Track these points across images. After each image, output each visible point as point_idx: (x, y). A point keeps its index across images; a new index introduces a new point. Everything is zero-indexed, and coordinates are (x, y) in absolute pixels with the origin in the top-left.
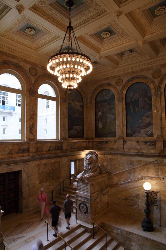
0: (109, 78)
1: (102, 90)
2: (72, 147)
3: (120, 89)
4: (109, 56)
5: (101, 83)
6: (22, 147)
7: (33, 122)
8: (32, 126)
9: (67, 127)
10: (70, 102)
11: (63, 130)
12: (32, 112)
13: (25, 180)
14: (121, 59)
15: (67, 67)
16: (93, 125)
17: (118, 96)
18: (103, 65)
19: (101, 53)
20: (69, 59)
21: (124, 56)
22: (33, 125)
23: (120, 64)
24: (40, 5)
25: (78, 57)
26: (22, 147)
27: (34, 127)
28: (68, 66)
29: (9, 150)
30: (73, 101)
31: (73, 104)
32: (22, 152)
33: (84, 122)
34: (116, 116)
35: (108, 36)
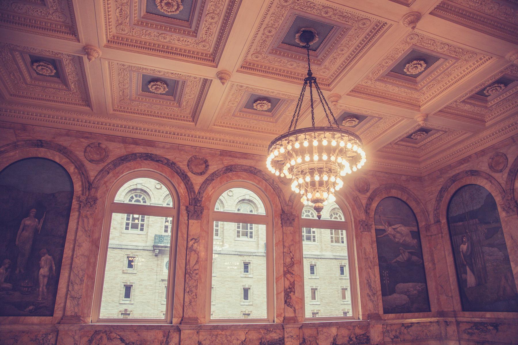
0: (470, 157)
1: (460, 189)
2: (396, 337)
3: (505, 179)
4: (445, 108)
5: (454, 173)
6: (268, 337)
7: (292, 281)
8: (290, 288)
9: (377, 285)
10: (381, 227)
11: (370, 296)
12: (288, 260)
14: (486, 107)
15: (304, 162)
16: (451, 279)
17: (503, 199)
18: (446, 132)
19: (422, 108)
20: (306, 144)
21: (488, 98)
22: (291, 287)
23: (486, 120)
24: (257, 59)
25: (325, 137)
26: (268, 337)
27: (294, 292)
28: (307, 158)
30: (390, 225)
31: (390, 230)
33: (426, 271)
34: (509, 250)
35: (420, 69)
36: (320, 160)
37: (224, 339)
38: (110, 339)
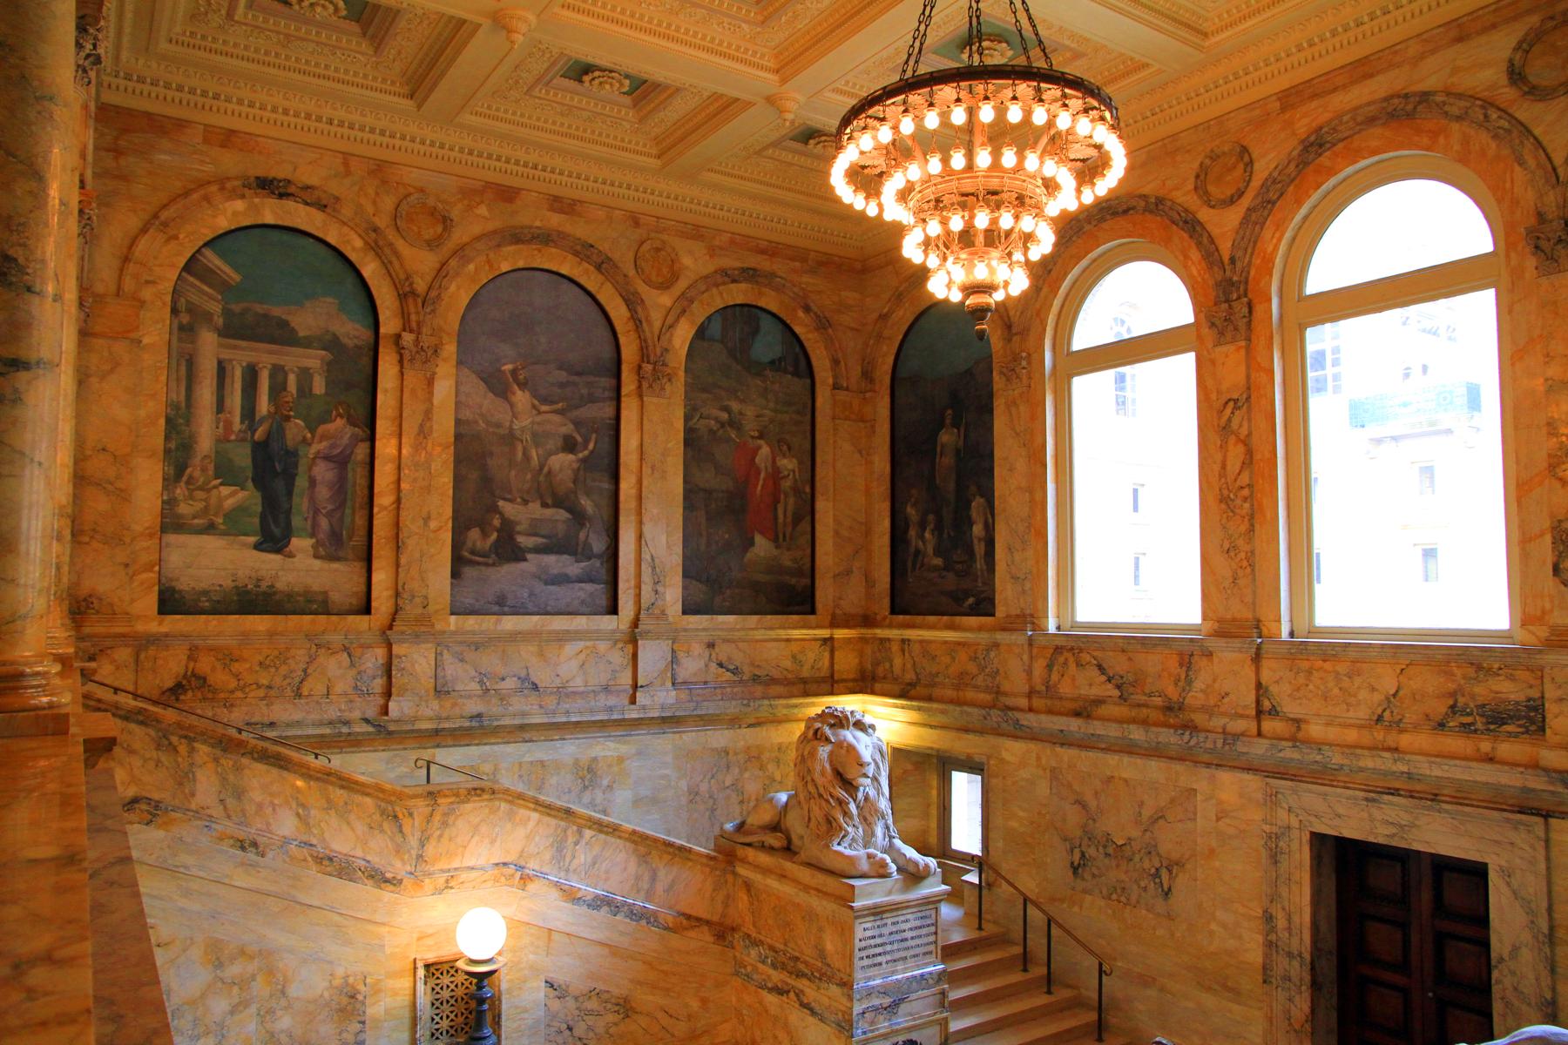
13: (1515, 949)
29: (1377, 697)
32: (1479, 726)
36: (996, 165)
37: (1331, 685)
38: (1079, 664)
